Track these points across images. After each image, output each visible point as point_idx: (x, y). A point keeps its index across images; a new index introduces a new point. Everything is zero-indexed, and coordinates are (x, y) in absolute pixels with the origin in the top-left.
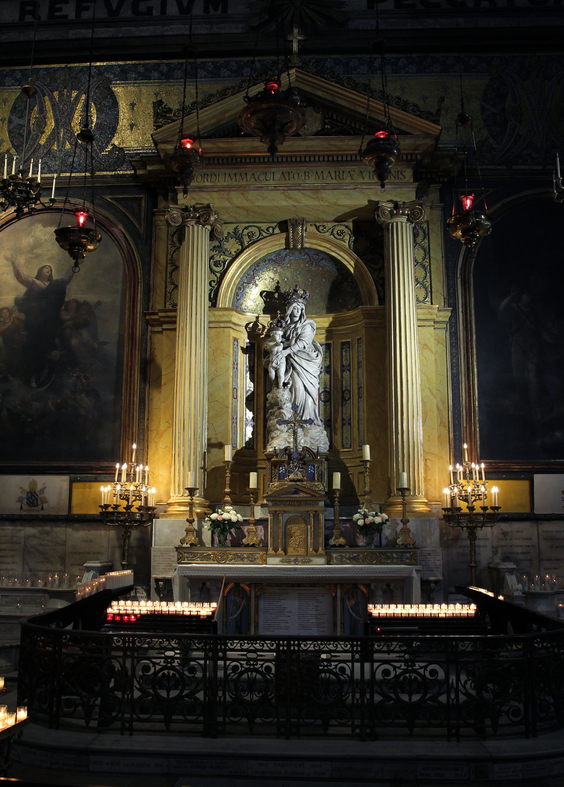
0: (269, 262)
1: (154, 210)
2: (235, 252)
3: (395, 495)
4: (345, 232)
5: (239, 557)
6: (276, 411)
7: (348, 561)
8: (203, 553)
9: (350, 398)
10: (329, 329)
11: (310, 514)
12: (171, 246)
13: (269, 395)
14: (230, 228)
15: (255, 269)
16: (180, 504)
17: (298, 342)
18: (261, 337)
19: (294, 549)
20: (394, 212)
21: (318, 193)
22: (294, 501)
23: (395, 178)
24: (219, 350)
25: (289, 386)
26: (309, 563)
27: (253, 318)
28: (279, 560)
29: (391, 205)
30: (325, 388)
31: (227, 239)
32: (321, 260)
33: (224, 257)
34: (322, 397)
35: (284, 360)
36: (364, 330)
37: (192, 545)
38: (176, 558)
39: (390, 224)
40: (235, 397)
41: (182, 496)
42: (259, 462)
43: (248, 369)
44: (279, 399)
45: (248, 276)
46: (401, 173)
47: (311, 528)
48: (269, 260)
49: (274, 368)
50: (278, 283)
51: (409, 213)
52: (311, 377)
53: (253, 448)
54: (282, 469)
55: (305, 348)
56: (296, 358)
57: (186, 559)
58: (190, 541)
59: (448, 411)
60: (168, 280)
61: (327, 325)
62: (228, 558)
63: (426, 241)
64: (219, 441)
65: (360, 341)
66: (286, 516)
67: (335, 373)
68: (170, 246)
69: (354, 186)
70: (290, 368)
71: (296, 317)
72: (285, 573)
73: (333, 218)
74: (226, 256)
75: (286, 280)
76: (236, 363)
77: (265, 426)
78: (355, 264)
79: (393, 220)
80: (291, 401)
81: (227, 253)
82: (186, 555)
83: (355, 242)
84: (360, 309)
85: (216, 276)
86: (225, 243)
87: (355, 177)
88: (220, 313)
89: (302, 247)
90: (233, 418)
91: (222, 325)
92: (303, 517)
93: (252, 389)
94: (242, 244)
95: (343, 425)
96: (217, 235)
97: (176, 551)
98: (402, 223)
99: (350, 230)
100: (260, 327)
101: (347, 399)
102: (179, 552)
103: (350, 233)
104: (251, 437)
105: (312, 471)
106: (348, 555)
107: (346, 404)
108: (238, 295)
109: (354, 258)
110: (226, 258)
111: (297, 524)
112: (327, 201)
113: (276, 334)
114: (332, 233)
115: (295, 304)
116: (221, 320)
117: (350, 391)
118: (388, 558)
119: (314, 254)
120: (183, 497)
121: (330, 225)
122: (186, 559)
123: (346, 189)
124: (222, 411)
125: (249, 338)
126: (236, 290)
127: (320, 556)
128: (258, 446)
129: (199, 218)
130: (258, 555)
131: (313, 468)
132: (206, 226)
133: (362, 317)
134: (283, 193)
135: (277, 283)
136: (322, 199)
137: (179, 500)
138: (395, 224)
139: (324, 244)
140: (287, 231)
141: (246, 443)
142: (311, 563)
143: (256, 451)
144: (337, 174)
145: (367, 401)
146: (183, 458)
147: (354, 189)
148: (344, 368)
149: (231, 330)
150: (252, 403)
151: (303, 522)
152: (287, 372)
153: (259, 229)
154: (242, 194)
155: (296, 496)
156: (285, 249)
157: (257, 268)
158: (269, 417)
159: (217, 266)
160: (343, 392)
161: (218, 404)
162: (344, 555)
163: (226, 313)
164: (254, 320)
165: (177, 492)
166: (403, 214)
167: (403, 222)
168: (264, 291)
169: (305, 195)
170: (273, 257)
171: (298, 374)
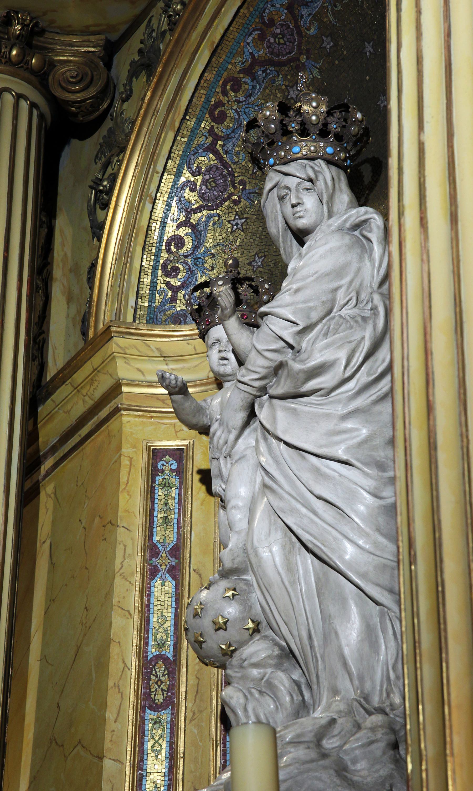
0: (254, 78)
15: (216, 138)
40: (159, 698)
96: (70, 97)
116: (98, 394)
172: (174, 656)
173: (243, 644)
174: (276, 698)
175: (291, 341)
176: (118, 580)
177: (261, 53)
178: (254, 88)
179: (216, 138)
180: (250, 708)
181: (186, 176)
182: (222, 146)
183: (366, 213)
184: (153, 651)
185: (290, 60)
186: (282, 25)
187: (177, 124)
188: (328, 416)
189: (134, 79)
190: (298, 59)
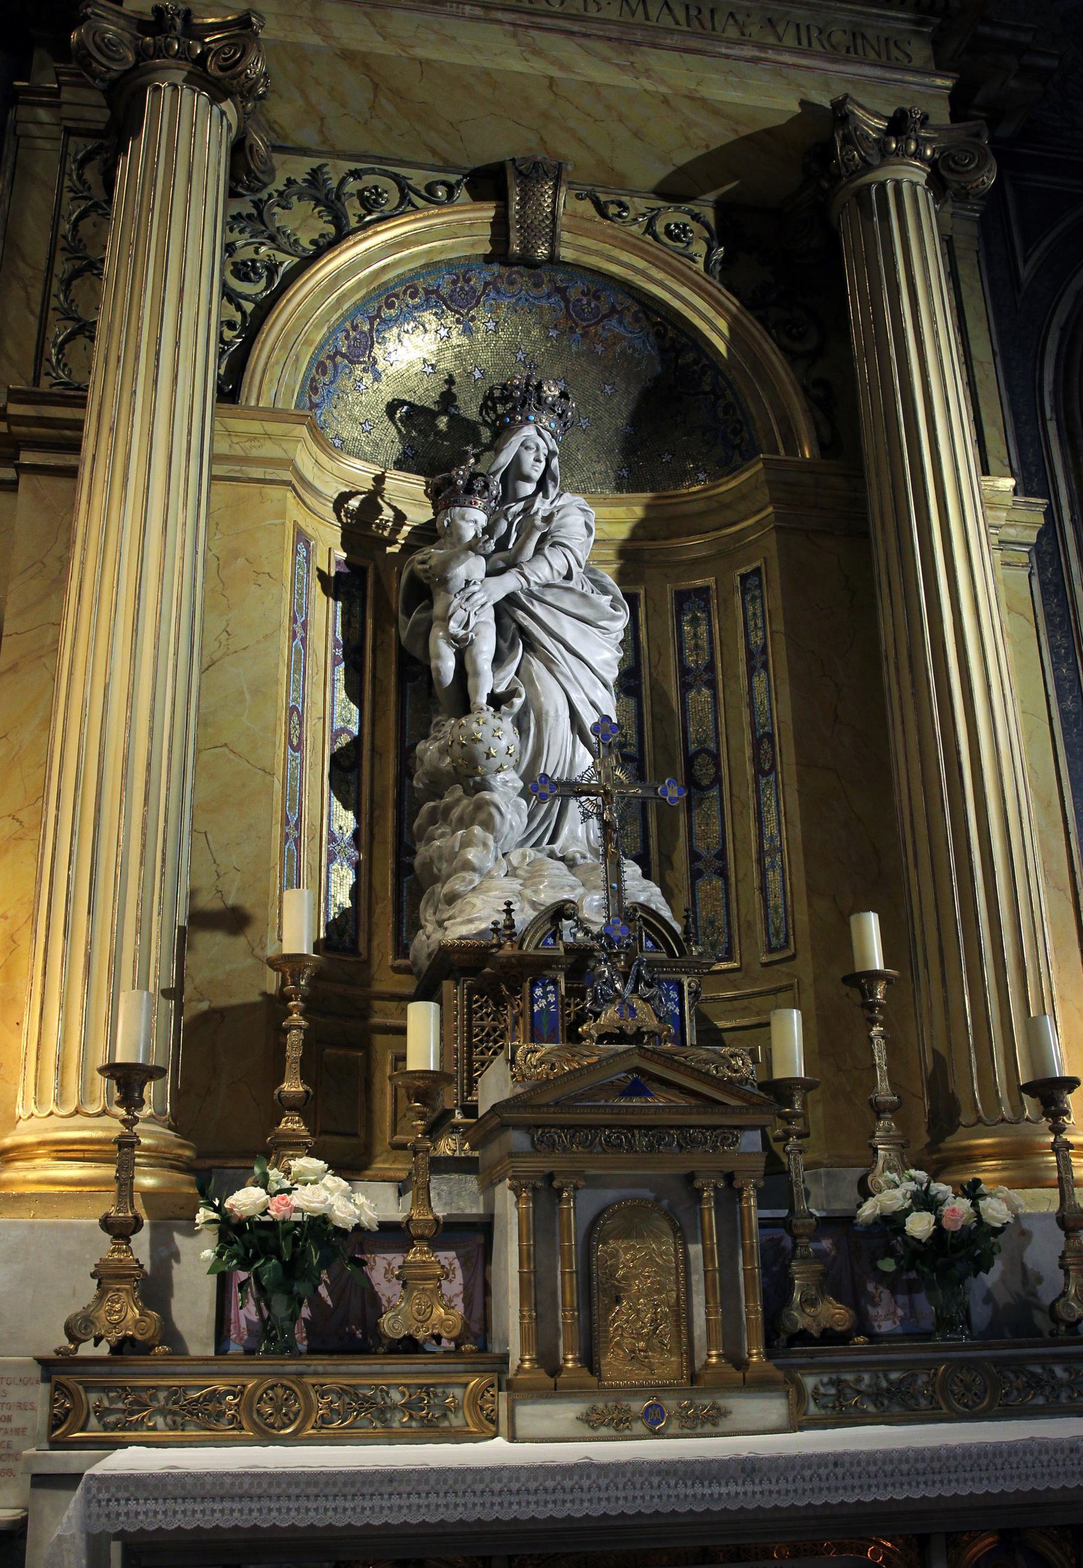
0: (427, 300)
1: (17, 83)
2: (313, 242)
3: (979, 1120)
4: (691, 231)
5: (366, 1404)
6: (458, 801)
7: (871, 1409)
8: (187, 1388)
9: (718, 780)
11: (700, 1191)
12: (72, 195)
13: (428, 750)
14: (299, 168)
15: (378, 316)
16: (64, 1150)
17: (546, 551)
18: (389, 550)
19: (633, 1356)
20: (890, 144)
21: (632, 54)
22: (631, 1128)
23: (879, 55)
24: (241, 561)
25: (518, 702)
26: (715, 1425)
27: (366, 480)
28: (572, 1415)
29: (882, 125)
33: (271, 252)
35: (489, 615)
36: (772, 543)
37: (124, 1347)
38: (40, 1416)
39: (874, 187)
40: (295, 742)
41: (77, 1112)
42: (377, 1004)
43: (339, 652)
44: (481, 748)
45: (352, 334)
46: (895, 43)
47: (707, 1253)
49: (453, 639)
50: (450, 381)
51: (937, 156)
52: (595, 684)
53: (354, 950)
54: (545, 996)
55: (569, 577)
56: (538, 609)
57: (93, 1421)
58: (115, 1325)
59: (1067, 833)
60: (54, 303)
61: (622, 532)
62: (309, 1409)
64: (231, 901)
65: (754, 581)
66: (590, 1201)
67: (660, 696)
68: (67, 196)
69: (756, 53)
70: (513, 646)
71: (527, 479)
72: (699, 1490)
73: (657, 174)
74: (279, 249)
75: (477, 375)
76: (300, 620)
77: (403, 869)
78: (731, 329)
79: (879, 175)
80: (516, 768)
81: (282, 240)
82: (93, 1398)
83: (725, 261)
84: (761, 465)
85: (239, 308)
86: (277, 210)
87: (754, 30)
88: (255, 427)
89: (553, 259)
90: (288, 823)
91: (257, 473)
92: (665, 1202)
93: (355, 730)
94: (338, 220)
95: (696, 875)
97: (46, 1379)
98: (914, 185)
99: (706, 226)
100: (387, 514)
101: (706, 782)
102: (58, 1387)
103: (707, 235)
104: (348, 904)
105: (671, 1006)
106: (866, 1377)
108: (315, 390)
109: (728, 311)
110: (280, 256)
111: (639, 1236)
112: (663, 81)
113: (463, 518)
115: (529, 431)
116: (255, 453)
117: (716, 757)
118: (1036, 1384)
119: (583, 293)
120: (79, 1120)
121: (639, 204)
122: (93, 1421)
123: (727, 57)
124: (244, 785)
125: (345, 545)
126: (309, 369)
127: (760, 1385)
128: (375, 943)
129: (201, 60)
130: (458, 1392)
131: (674, 995)
133: (764, 495)
134: (514, 36)
135: (446, 381)
136: (648, 73)
137: (58, 1129)
138: (890, 186)
139: (625, 257)
140: (501, 196)
141: (328, 926)
142: (725, 1424)
143: (368, 963)
144: (693, 12)
145: (801, 781)
146: (90, 943)
147: (755, 60)
148: (689, 679)
149: (290, 495)
150: (351, 777)
151: (665, 1226)
152: (499, 660)
153: (399, 184)
154: (366, 14)
155: (636, 1102)
156: (488, 259)
157: (386, 313)
158: (422, 829)
159: (245, 278)
160: (689, 760)
161: (232, 756)
162: (849, 1377)
163: (273, 428)
164: (369, 485)
165: (51, 1092)
166: (918, 155)
168: (403, 403)
169: (587, 51)
171: (549, 663)
178: (422, 305)
186: (472, 288)
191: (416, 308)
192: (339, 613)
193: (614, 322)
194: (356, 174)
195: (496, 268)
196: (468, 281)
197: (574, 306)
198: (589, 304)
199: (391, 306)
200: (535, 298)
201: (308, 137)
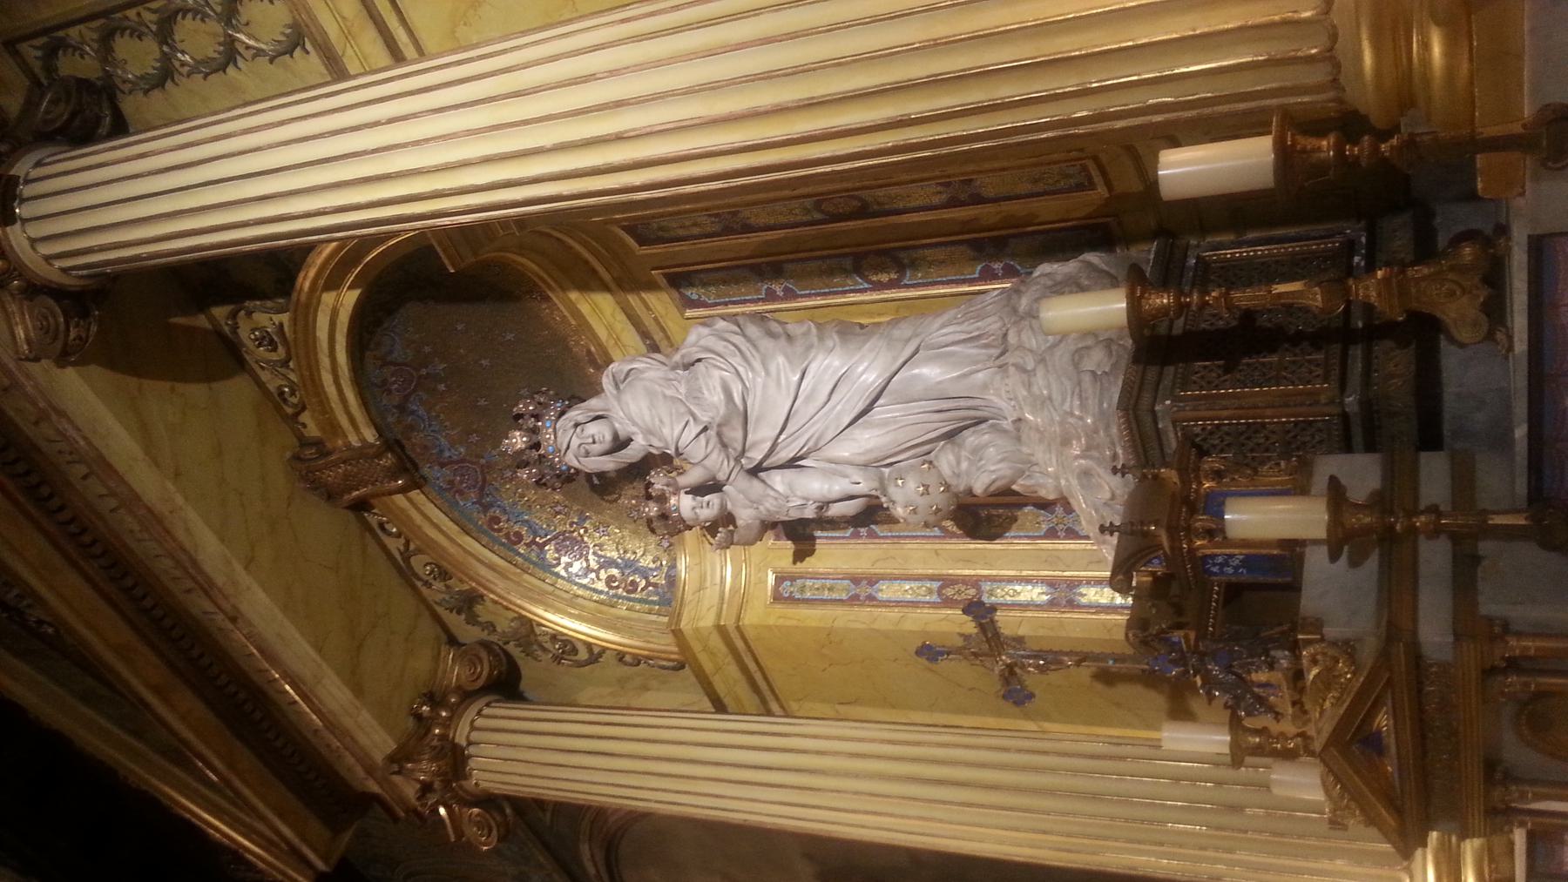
0: (491, 505)
10: (613, 285)
15: (533, 542)
30: (846, 272)
31: (491, 627)
32: (395, 364)
34: (884, 278)
43: (863, 531)
48: (486, 508)
52: (808, 399)
55: (705, 429)
63: (73, 32)
76: (854, 590)
95: (978, 200)
96: (485, 673)
101: (855, 203)
107: (878, 204)
114: (285, 363)
132: (464, 743)
167: (29, 238)
170: (468, 503)
172: (939, 580)
173: (940, 475)
174: (986, 446)
175: (701, 427)
176: (876, 626)
177: (473, 496)
178: (499, 506)
179: (533, 542)
180: (993, 468)
181: (560, 570)
182: (541, 538)
183: (607, 376)
184: (935, 598)
185: (482, 472)
187: (519, 571)
188: (765, 386)
189: (480, 619)
190: (482, 466)
191: (504, 511)
192: (825, 534)
193: (395, 355)
194: (427, 584)
195: (425, 470)
196: (451, 483)
197: (405, 389)
198: (395, 382)
199: (519, 537)
200: (424, 420)
201: (427, 628)
